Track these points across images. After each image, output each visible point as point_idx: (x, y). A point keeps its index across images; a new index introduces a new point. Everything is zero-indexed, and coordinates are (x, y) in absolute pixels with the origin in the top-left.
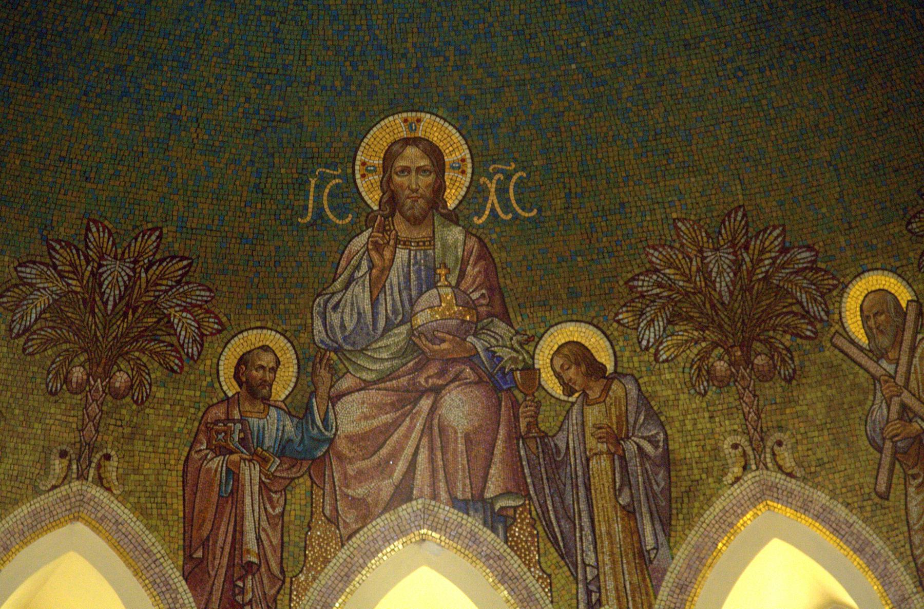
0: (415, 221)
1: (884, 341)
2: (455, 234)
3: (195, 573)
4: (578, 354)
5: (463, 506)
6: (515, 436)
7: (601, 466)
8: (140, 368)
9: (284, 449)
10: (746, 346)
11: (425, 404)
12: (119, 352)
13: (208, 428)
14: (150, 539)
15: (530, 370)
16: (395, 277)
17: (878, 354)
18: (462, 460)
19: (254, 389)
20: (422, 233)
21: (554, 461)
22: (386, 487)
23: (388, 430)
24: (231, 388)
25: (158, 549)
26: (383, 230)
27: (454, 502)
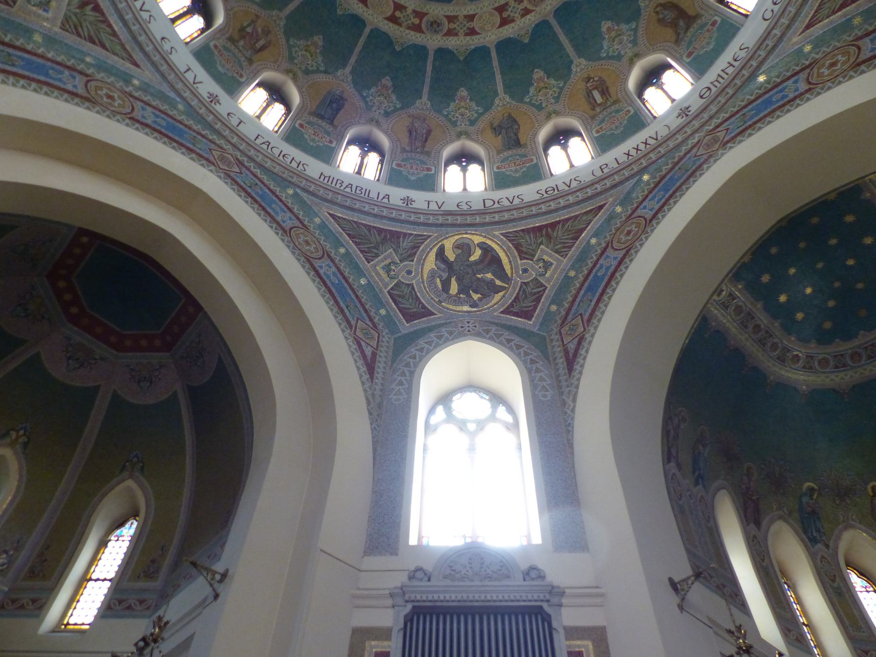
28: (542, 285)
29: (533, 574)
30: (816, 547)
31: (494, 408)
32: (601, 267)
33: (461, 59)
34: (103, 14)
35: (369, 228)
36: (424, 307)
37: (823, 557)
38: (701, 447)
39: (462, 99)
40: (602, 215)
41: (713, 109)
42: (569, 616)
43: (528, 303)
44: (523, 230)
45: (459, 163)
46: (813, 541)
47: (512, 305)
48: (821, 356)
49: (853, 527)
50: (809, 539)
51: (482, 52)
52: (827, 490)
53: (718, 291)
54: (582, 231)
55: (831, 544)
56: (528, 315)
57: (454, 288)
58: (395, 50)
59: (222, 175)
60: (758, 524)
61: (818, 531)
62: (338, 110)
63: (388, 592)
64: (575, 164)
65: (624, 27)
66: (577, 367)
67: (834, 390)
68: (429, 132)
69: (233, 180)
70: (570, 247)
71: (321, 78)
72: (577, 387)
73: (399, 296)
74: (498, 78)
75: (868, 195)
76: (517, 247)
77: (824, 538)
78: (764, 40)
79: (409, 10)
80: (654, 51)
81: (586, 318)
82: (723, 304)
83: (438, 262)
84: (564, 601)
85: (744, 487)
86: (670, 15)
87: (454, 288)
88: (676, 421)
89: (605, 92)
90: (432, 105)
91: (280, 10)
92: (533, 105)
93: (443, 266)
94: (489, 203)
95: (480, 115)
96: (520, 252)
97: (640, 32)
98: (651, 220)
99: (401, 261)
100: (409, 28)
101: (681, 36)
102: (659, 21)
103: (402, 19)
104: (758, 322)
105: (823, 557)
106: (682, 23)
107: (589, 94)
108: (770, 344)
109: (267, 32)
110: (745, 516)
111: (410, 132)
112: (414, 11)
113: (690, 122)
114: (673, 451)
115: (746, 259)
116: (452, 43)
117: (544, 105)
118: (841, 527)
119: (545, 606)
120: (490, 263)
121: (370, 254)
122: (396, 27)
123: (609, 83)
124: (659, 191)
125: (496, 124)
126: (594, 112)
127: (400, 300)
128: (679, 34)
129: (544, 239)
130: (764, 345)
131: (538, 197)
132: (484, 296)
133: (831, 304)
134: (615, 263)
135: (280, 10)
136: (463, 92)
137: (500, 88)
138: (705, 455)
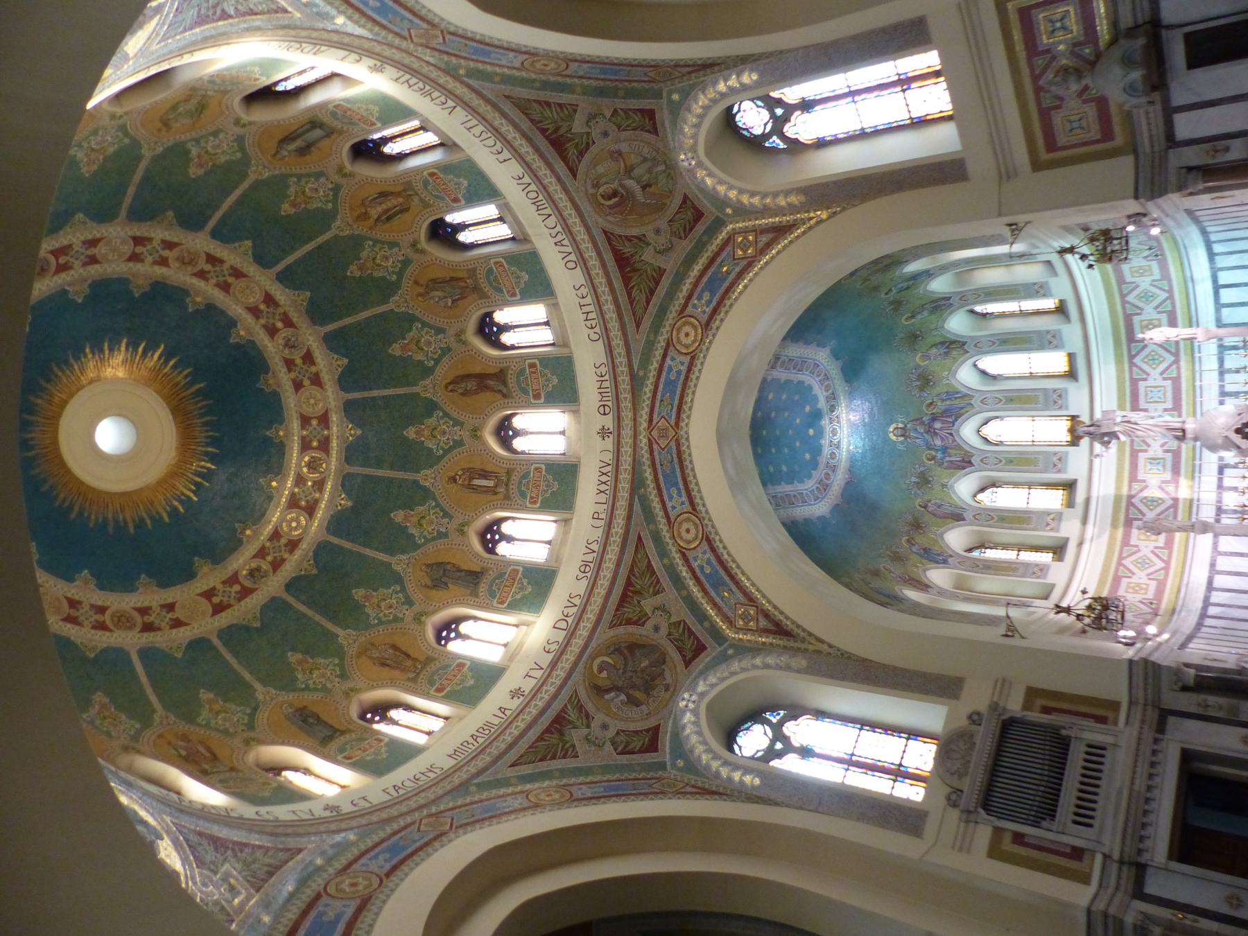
19: (933, 458)
28: (679, 623)
29: (975, 717)
31: (766, 722)
32: (702, 568)
33: (315, 571)
34: (246, 845)
35: (541, 738)
36: (648, 730)
39: (366, 597)
40: (649, 544)
41: (627, 415)
42: (1015, 705)
43: (689, 644)
44: (617, 610)
45: (448, 639)
46: (945, 562)
47: (684, 656)
51: (322, 551)
54: (649, 565)
56: (700, 648)
57: (639, 695)
58: (257, 629)
59: (461, 831)
60: (927, 586)
62: (318, 718)
63: (963, 825)
64: (549, 538)
65: (431, 421)
66: (791, 626)
68: (395, 647)
69: (467, 824)
70: (658, 581)
71: (262, 717)
72: (810, 634)
73: (626, 747)
74: (368, 552)
76: (629, 622)
78: (611, 351)
79: (220, 587)
80: (488, 416)
81: (742, 599)
83: (607, 697)
84: (1001, 705)
86: (471, 385)
87: (639, 695)
89: (484, 475)
90: (355, 629)
91: (154, 711)
92: (433, 539)
93: (612, 694)
94: (563, 625)
95: (403, 590)
96: (635, 623)
97: (455, 415)
98: (694, 509)
99: (588, 726)
100: (240, 600)
101: (505, 391)
102: (462, 394)
103: (225, 599)
106: (491, 383)
107: (471, 487)
109: (185, 737)
111: (383, 665)
112: (224, 583)
113: (619, 435)
116: (289, 570)
117: (443, 530)
119: (1003, 717)
120: (632, 653)
121: (569, 752)
122: (229, 611)
123: (477, 465)
124: (668, 490)
125: (429, 583)
126: (500, 496)
127: (631, 747)
128: (500, 391)
129: (636, 598)
131: (584, 583)
132: (662, 674)
134: (709, 555)
135: (154, 711)
136: (359, 593)
137: (383, 557)
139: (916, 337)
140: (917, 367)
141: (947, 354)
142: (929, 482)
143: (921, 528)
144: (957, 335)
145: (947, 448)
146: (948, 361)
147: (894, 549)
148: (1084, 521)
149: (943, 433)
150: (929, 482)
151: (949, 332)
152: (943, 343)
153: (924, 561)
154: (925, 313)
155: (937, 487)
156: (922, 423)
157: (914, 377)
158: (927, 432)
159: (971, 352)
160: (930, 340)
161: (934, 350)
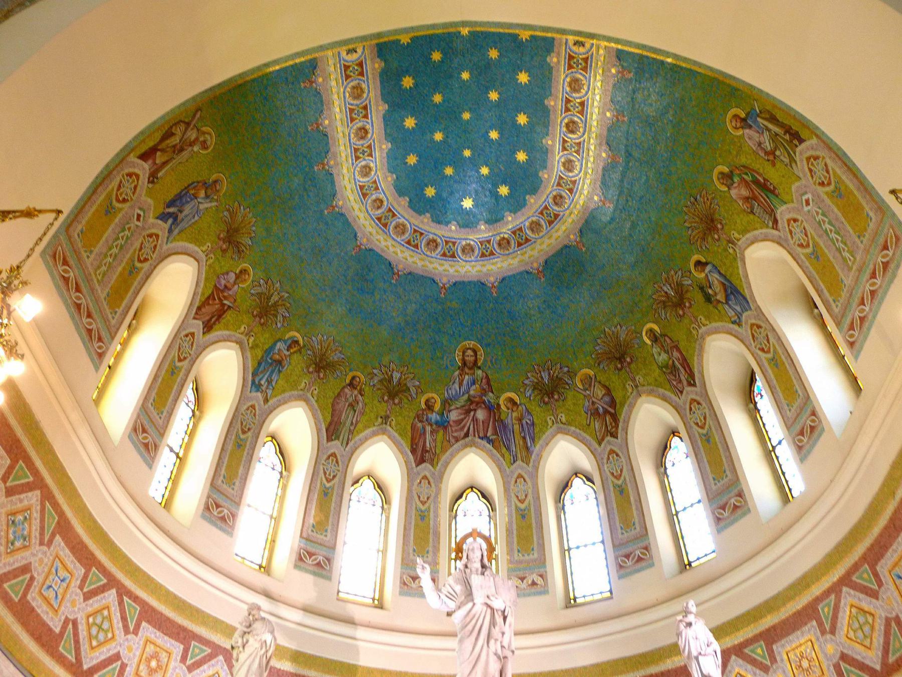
0: (470, 369)
1: (587, 386)
2: (480, 372)
3: (413, 451)
4: (511, 400)
5: (482, 439)
6: (495, 420)
7: (516, 427)
8: (401, 399)
9: (437, 423)
10: (552, 394)
11: (472, 413)
12: (396, 394)
13: (418, 416)
14: (402, 442)
15: (499, 405)
16: (465, 382)
17: (585, 390)
18: (481, 427)
19: (429, 407)
20: (472, 371)
21: (505, 427)
22: (462, 434)
23: (462, 420)
24: (424, 406)
25: (404, 445)
26: (462, 370)
27: (479, 437)
30: (254, 394)
37: (253, 407)
38: (202, 194)
46: (256, 386)
48: (402, 220)
49: (307, 401)
50: (253, 382)
52: (309, 352)
53: (350, 45)
55: (271, 402)
60: (208, 327)
61: (269, 382)
67: (390, 264)
75: (555, 60)
77: (269, 392)
82: (347, 67)
85: (223, 282)
88: (192, 135)
104: (368, 127)
105: (253, 407)
108: (363, 163)
110: (199, 308)
114: (160, 158)
115: (405, 39)
118: (296, 392)
130: (357, 158)
133: (449, 171)
138: (201, 207)
139: (621, 359)
140: (572, 374)
141: (595, 413)
142: (392, 396)
143: (318, 372)
144: (627, 422)
145: (445, 428)
146: (583, 419)
147: (281, 310)
148: (307, 609)
149: (468, 422)
150: (392, 396)
151: (632, 406)
152: (613, 403)
153: (259, 353)
154: (663, 358)
155: (382, 409)
156: (484, 392)
157: (555, 372)
158: (470, 400)
159: (599, 449)
160: (615, 381)
161: (600, 392)
